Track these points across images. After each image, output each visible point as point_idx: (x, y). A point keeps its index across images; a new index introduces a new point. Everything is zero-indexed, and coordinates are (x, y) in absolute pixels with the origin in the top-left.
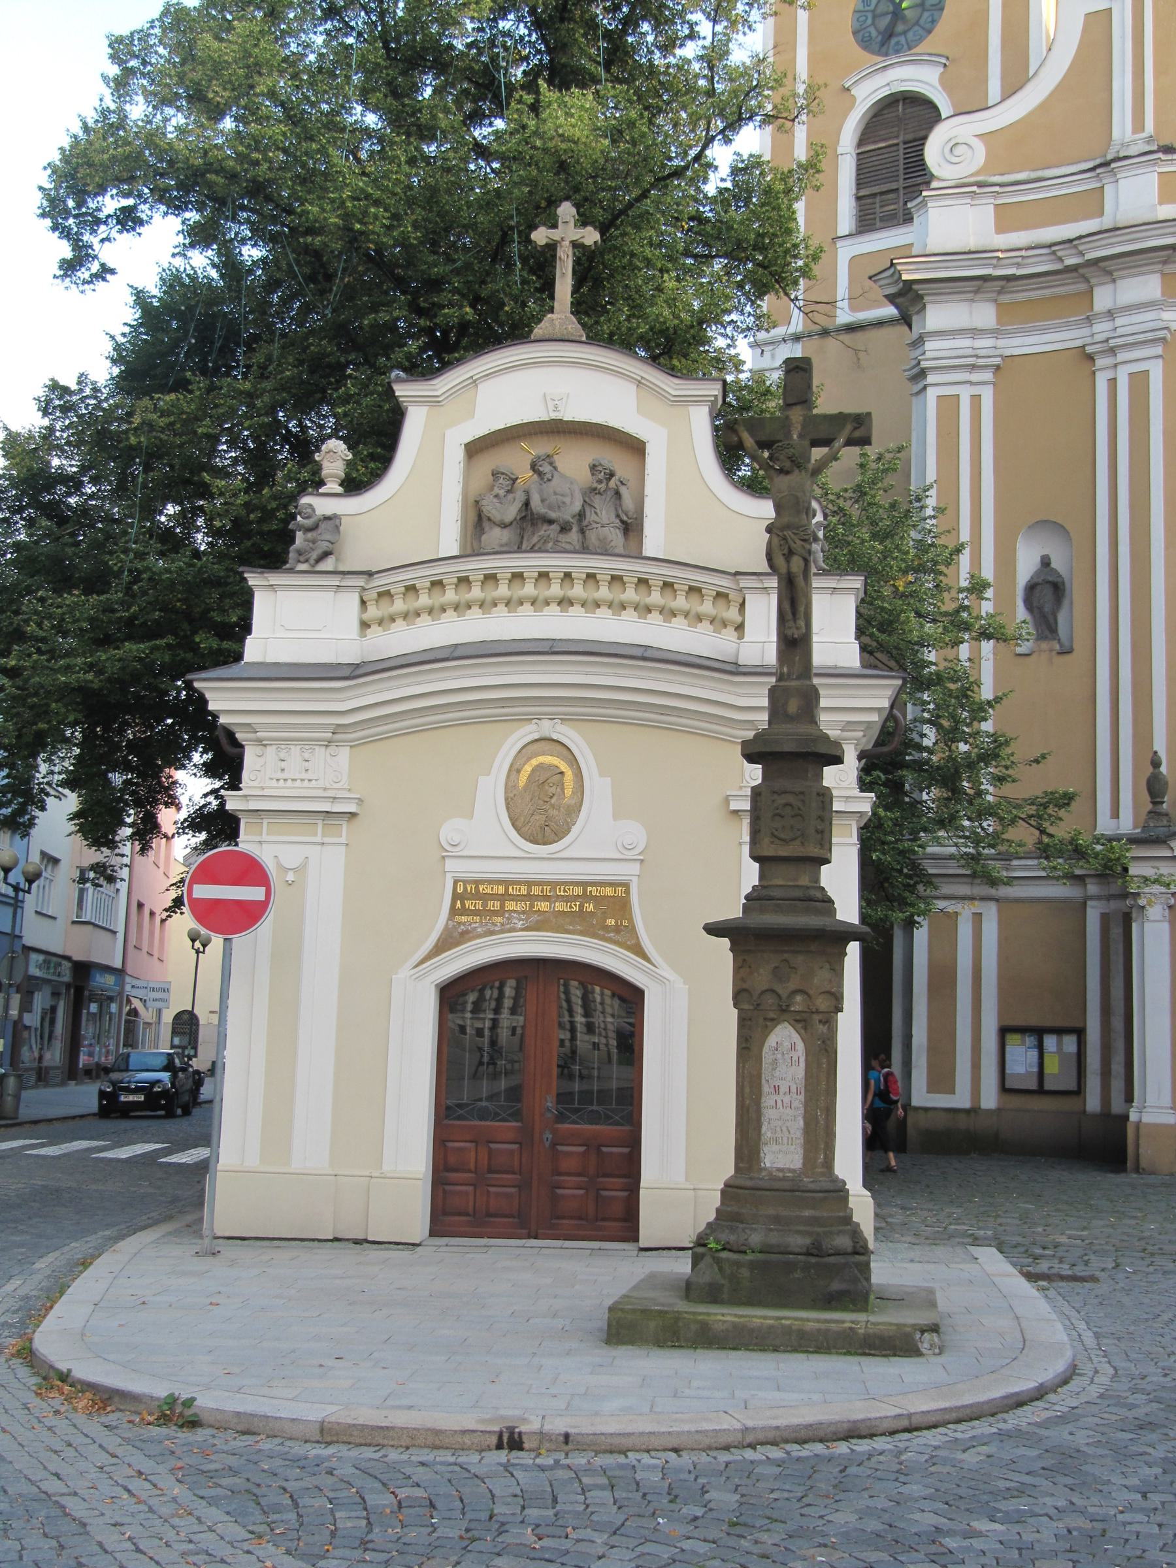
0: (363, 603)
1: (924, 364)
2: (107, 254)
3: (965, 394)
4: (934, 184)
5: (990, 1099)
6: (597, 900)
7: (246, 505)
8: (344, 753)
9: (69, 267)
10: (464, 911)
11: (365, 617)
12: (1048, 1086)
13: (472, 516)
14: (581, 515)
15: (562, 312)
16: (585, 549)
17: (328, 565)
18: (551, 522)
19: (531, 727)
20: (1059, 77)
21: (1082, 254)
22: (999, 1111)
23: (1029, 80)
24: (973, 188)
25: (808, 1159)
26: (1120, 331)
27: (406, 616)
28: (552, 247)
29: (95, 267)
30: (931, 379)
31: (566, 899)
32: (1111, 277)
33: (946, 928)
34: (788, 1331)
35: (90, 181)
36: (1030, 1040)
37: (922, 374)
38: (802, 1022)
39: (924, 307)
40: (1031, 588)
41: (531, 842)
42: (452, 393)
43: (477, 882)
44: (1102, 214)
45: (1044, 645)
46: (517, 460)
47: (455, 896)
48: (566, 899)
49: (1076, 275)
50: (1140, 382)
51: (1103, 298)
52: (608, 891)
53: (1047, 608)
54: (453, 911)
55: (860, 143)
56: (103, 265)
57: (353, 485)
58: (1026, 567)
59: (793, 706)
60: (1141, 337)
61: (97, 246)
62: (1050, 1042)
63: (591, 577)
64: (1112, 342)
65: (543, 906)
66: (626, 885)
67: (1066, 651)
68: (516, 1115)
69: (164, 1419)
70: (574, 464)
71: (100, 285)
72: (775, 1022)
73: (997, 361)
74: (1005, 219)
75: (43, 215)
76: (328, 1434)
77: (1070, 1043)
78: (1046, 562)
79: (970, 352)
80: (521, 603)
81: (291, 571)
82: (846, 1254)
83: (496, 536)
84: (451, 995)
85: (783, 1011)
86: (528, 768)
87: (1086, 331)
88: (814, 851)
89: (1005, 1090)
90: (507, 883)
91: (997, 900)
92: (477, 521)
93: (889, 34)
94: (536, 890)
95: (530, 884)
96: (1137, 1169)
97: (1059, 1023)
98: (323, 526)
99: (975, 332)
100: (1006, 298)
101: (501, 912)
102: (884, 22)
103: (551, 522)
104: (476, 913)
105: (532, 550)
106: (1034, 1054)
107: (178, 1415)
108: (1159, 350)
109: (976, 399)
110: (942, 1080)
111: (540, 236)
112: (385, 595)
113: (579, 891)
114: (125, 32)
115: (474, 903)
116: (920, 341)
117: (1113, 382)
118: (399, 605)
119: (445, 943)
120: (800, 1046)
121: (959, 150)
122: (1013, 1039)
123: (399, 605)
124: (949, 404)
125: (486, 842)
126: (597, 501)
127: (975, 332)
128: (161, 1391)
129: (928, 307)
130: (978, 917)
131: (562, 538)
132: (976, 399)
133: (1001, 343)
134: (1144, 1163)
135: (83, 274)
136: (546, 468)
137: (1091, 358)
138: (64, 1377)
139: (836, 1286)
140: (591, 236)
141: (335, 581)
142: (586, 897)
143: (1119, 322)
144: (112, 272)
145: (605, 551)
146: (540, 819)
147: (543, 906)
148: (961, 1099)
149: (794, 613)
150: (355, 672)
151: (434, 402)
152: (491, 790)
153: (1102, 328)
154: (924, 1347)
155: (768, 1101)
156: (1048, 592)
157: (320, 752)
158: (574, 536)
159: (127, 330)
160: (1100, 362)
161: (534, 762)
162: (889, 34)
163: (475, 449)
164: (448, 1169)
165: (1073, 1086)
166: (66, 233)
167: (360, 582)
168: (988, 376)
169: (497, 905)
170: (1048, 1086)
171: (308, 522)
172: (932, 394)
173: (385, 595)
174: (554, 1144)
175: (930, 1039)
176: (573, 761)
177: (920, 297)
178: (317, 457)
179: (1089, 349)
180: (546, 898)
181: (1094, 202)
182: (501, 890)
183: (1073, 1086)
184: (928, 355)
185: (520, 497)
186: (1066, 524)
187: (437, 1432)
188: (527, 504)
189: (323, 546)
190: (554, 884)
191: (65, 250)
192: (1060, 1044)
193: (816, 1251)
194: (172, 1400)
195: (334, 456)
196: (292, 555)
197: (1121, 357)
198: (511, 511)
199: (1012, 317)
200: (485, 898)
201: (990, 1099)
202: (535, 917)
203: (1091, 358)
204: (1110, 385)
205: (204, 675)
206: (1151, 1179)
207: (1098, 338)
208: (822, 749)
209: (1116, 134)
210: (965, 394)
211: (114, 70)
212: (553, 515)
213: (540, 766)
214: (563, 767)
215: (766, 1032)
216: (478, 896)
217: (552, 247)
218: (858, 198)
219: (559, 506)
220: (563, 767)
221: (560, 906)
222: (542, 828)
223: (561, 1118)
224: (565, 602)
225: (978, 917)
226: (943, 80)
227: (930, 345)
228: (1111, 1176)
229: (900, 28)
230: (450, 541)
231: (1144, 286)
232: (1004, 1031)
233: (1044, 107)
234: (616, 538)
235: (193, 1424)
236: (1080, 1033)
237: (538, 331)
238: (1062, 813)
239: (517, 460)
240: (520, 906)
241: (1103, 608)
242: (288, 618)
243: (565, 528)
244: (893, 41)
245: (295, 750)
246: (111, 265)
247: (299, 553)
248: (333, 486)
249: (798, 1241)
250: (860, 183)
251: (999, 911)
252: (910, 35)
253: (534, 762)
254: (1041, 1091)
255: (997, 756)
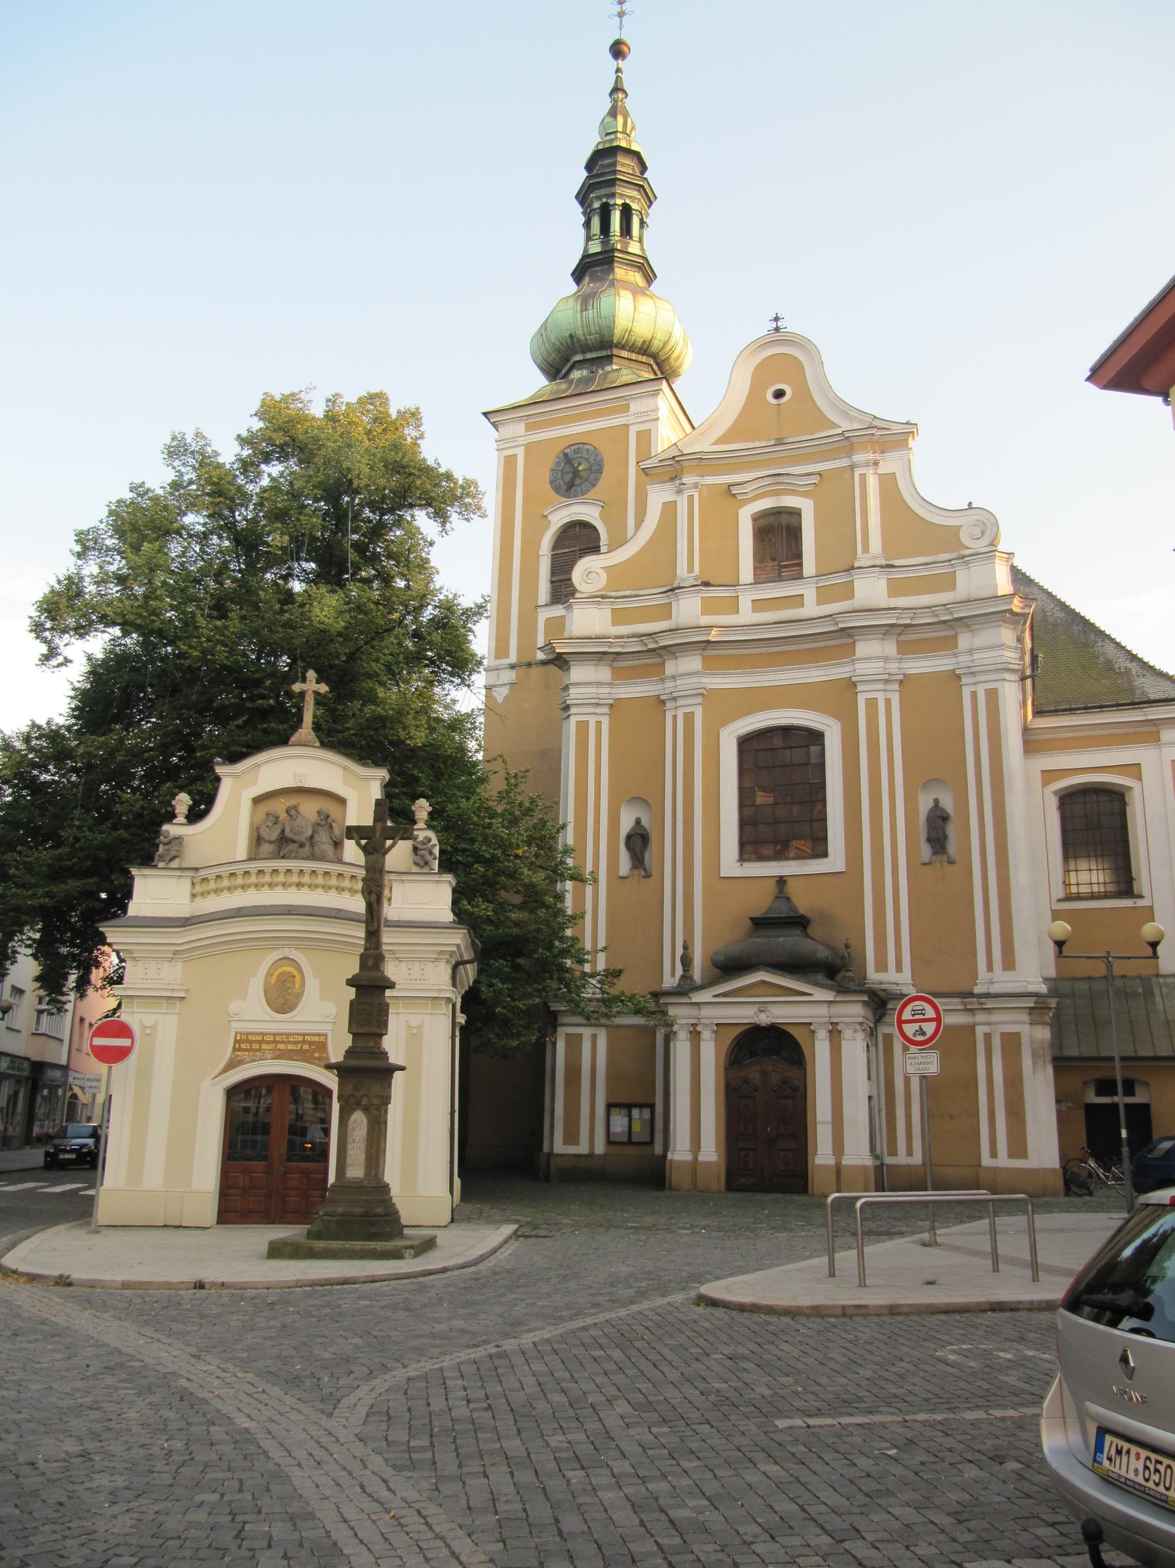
0: (193, 884)
1: (568, 702)
2: (67, 652)
3: (592, 721)
4: (577, 595)
5: (600, 1148)
6: (310, 1043)
7: (142, 807)
8: (179, 966)
9: (46, 658)
10: (240, 1049)
11: (194, 891)
12: (634, 1139)
13: (255, 838)
14: (312, 837)
15: (306, 730)
16: (313, 857)
17: (175, 864)
18: (294, 842)
19: (279, 952)
20: (644, 542)
21: (657, 642)
22: (605, 1156)
23: (626, 542)
24: (600, 598)
25: (367, 1173)
26: (679, 688)
27: (216, 891)
28: (302, 694)
29: (60, 659)
30: (573, 710)
31: (294, 1043)
32: (674, 655)
33: (574, 1043)
34: (347, 1250)
35: (62, 611)
36: (624, 1111)
37: (567, 708)
38: (366, 1110)
39: (569, 668)
40: (629, 837)
41: (279, 1012)
42: (245, 772)
43: (248, 1034)
44: (670, 618)
45: (636, 872)
46: (279, 806)
47: (236, 1041)
48: (294, 1043)
49: (653, 656)
50: (689, 717)
51: (671, 667)
52: (316, 1039)
53: (638, 849)
54: (234, 1049)
55: (554, 548)
56: (65, 658)
57: (195, 815)
58: (626, 825)
59: (370, 963)
60: (315, 936)
61: (62, 647)
62: (636, 1113)
63: (314, 872)
64: (675, 694)
65: (282, 1046)
66: (325, 1035)
67: (648, 875)
68: (265, 1158)
69: (57, 1284)
70: (309, 809)
71: (63, 668)
72: (354, 1110)
73: (611, 702)
74: (618, 617)
75: (31, 631)
76: (126, 1285)
77: (646, 1113)
78: (638, 822)
79: (595, 696)
80: (277, 885)
81: (155, 867)
82: (381, 1216)
83: (267, 848)
84: (232, 1093)
85: (358, 1105)
86: (277, 973)
87: (660, 686)
88: (375, 1030)
89: (609, 1142)
90: (263, 1034)
91: (606, 1026)
92: (257, 840)
93: (571, 485)
94: (278, 1038)
95: (275, 1035)
96: (671, 1188)
97: (640, 1101)
98: (173, 842)
99: (599, 684)
100: (615, 664)
101: (259, 1050)
102: (568, 477)
103: (294, 842)
104: (246, 1050)
105: (283, 857)
106: (626, 1120)
107: (64, 1282)
108: (700, 700)
109: (599, 723)
110: (572, 1136)
111: (297, 687)
112: (205, 880)
113: (301, 1038)
114: (85, 528)
115: (246, 1045)
116: (566, 688)
117: (675, 717)
118: (212, 885)
119: (231, 1065)
120: (365, 1121)
121: (592, 576)
122: (614, 1111)
123: (212, 885)
124: (583, 727)
125: (252, 1012)
126: (320, 830)
127: (599, 684)
128: (57, 1273)
129: (572, 668)
130: (594, 1036)
131: (301, 850)
132: (599, 723)
133: (613, 691)
134: (673, 1185)
135: (54, 662)
136: (293, 813)
137: (663, 702)
138: (14, 1272)
139: (374, 1230)
140: (323, 688)
141: (178, 873)
142: (304, 1042)
143: (679, 682)
144: (71, 661)
145: (323, 858)
146: (281, 1000)
147: (282, 1046)
148: (582, 1148)
149: (372, 919)
150: (185, 922)
151: (236, 776)
152: (256, 986)
153: (669, 684)
154: (406, 1255)
155: (350, 1146)
156: (639, 840)
157: (166, 964)
158: (307, 849)
159: (81, 679)
160: (669, 705)
161: (280, 970)
162: (571, 485)
163: (257, 801)
164: (228, 1187)
165: (648, 1140)
166: (45, 641)
167: (191, 873)
168: (606, 710)
169: (257, 1046)
170: (634, 1139)
171: (166, 840)
172: (573, 720)
173: (205, 880)
174: (285, 1173)
175: (565, 1112)
176: (300, 970)
177: (566, 662)
178: (173, 802)
179: (662, 697)
180: (283, 1042)
181: (665, 612)
182: (260, 1038)
183: (648, 1140)
184: (572, 696)
185: (279, 827)
186: (649, 799)
187: (170, 1283)
188: (283, 831)
189: (173, 853)
190: (288, 1035)
191: (44, 649)
192: (641, 1113)
193: (365, 1215)
194: (61, 1276)
195: (183, 802)
196: (156, 858)
197: (680, 702)
198: (275, 835)
199: (620, 675)
200: (251, 1042)
201: (600, 1148)
202: (277, 1053)
203: (663, 702)
204: (674, 717)
205: (105, 924)
206: (675, 1193)
207: (668, 691)
208: (380, 984)
209: (678, 573)
210: (592, 721)
211: (78, 548)
212: (295, 838)
213: (282, 973)
214: (295, 972)
215: (350, 1114)
216: (247, 1041)
217: (302, 694)
218: (552, 582)
219: (300, 833)
220: (295, 972)
221: (290, 1047)
222: (283, 1005)
223: (289, 1159)
224: (299, 885)
225: (594, 1036)
226: (601, 514)
227: (572, 691)
228: (655, 1193)
229: (577, 481)
230: (242, 851)
231: (692, 663)
232: (610, 1106)
233: (640, 553)
234: (329, 849)
235: (70, 1285)
236: (652, 1106)
237: (293, 739)
238: (615, 981)
239: (279, 806)
240: (269, 1047)
241: (668, 849)
242: (153, 892)
243: (302, 845)
244: (573, 489)
245: (153, 964)
246: (70, 658)
247: (160, 856)
248: (181, 819)
249: (358, 1210)
250: (553, 573)
251: (608, 1033)
252: (583, 486)
253: (280, 970)
254: (630, 1142)
255: (569, 952)
